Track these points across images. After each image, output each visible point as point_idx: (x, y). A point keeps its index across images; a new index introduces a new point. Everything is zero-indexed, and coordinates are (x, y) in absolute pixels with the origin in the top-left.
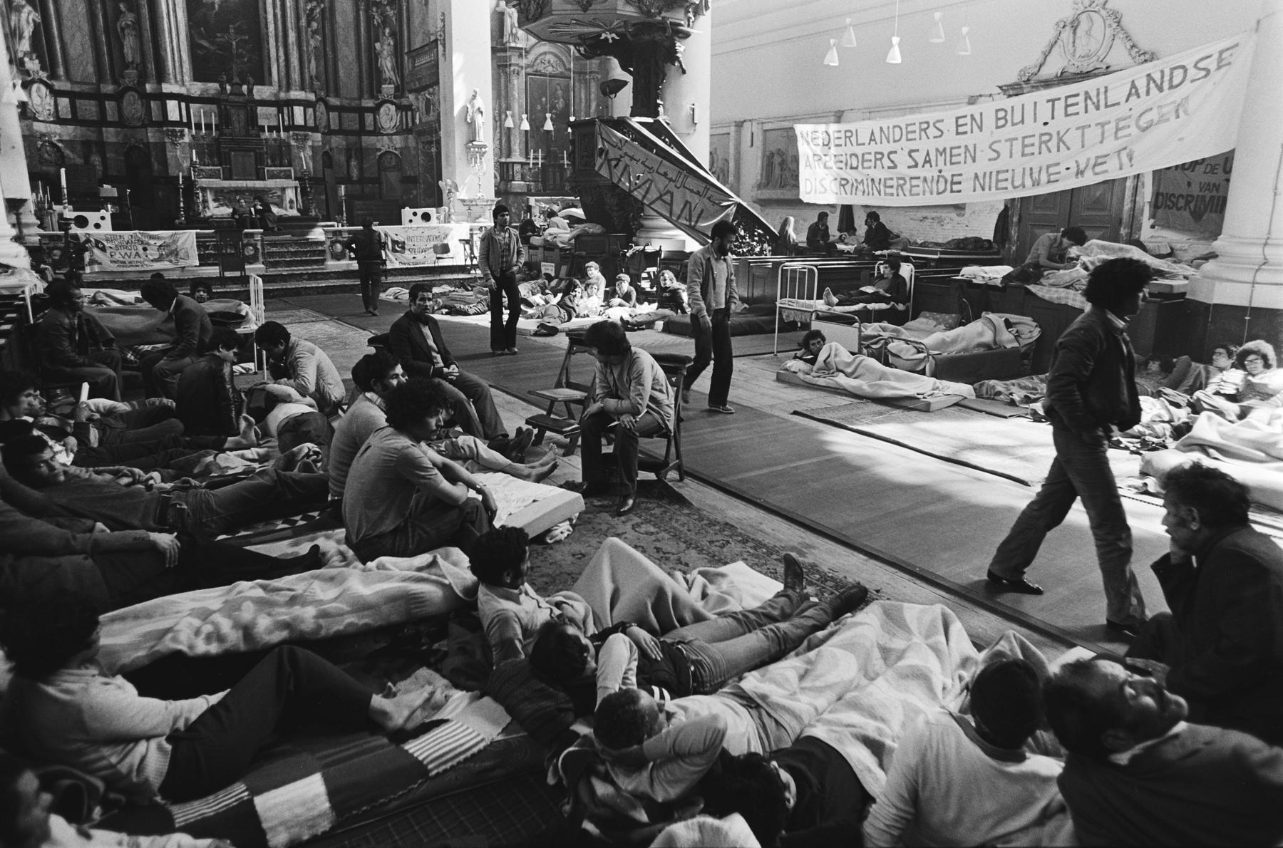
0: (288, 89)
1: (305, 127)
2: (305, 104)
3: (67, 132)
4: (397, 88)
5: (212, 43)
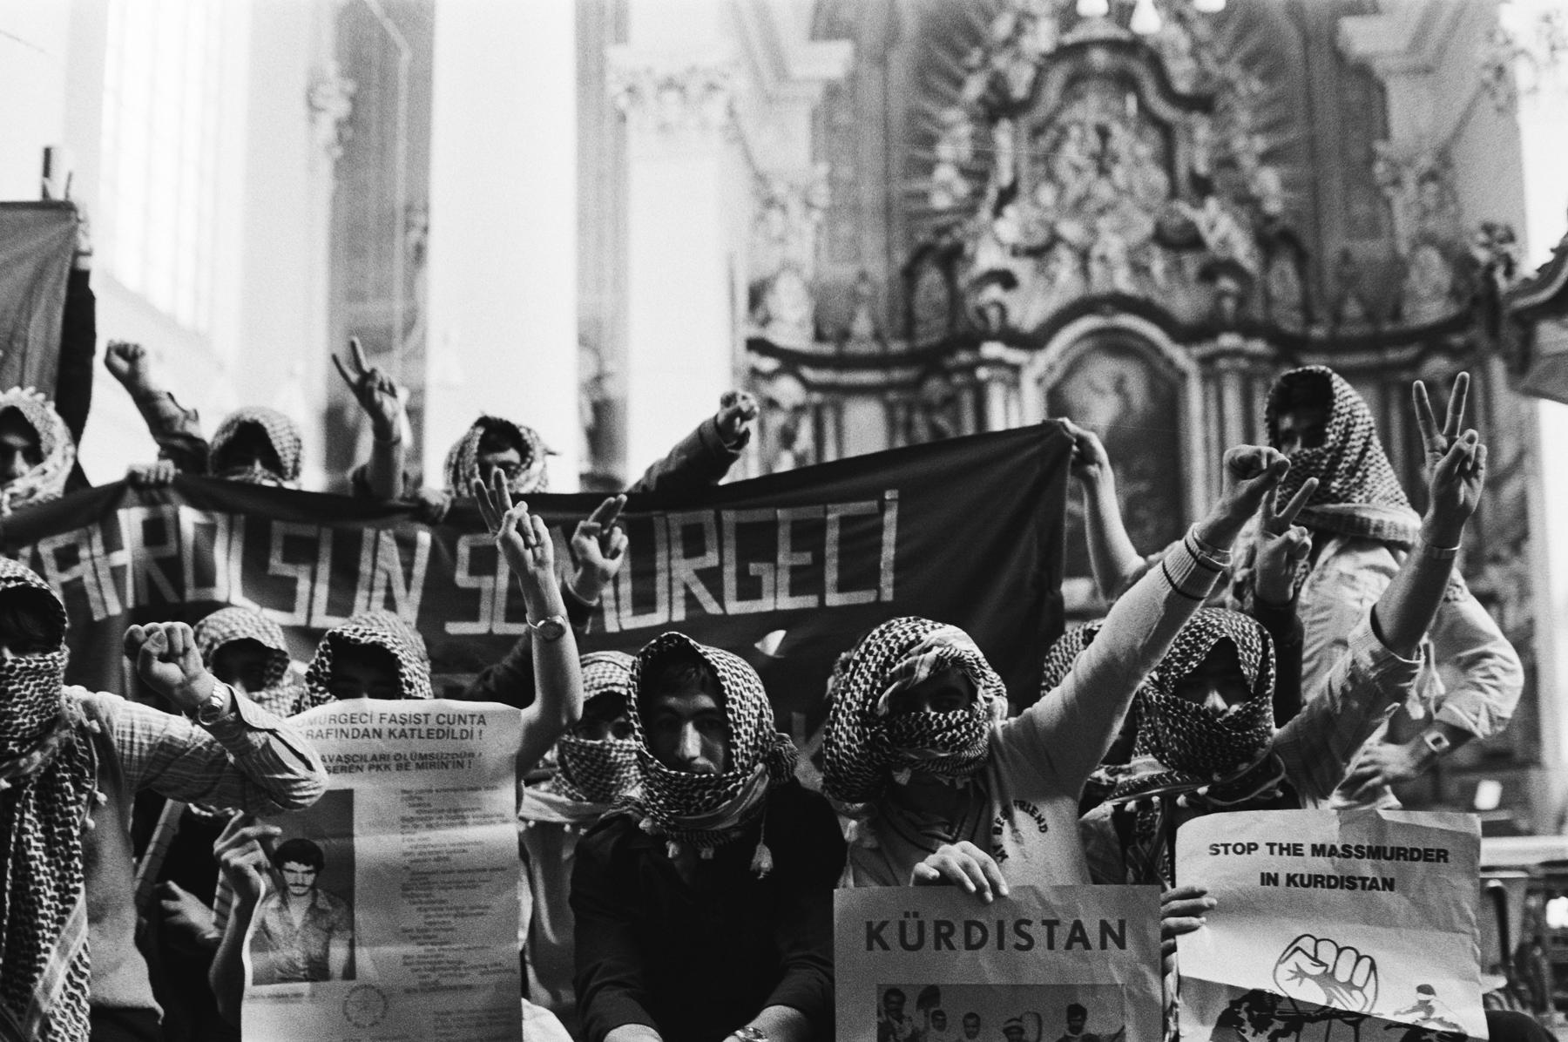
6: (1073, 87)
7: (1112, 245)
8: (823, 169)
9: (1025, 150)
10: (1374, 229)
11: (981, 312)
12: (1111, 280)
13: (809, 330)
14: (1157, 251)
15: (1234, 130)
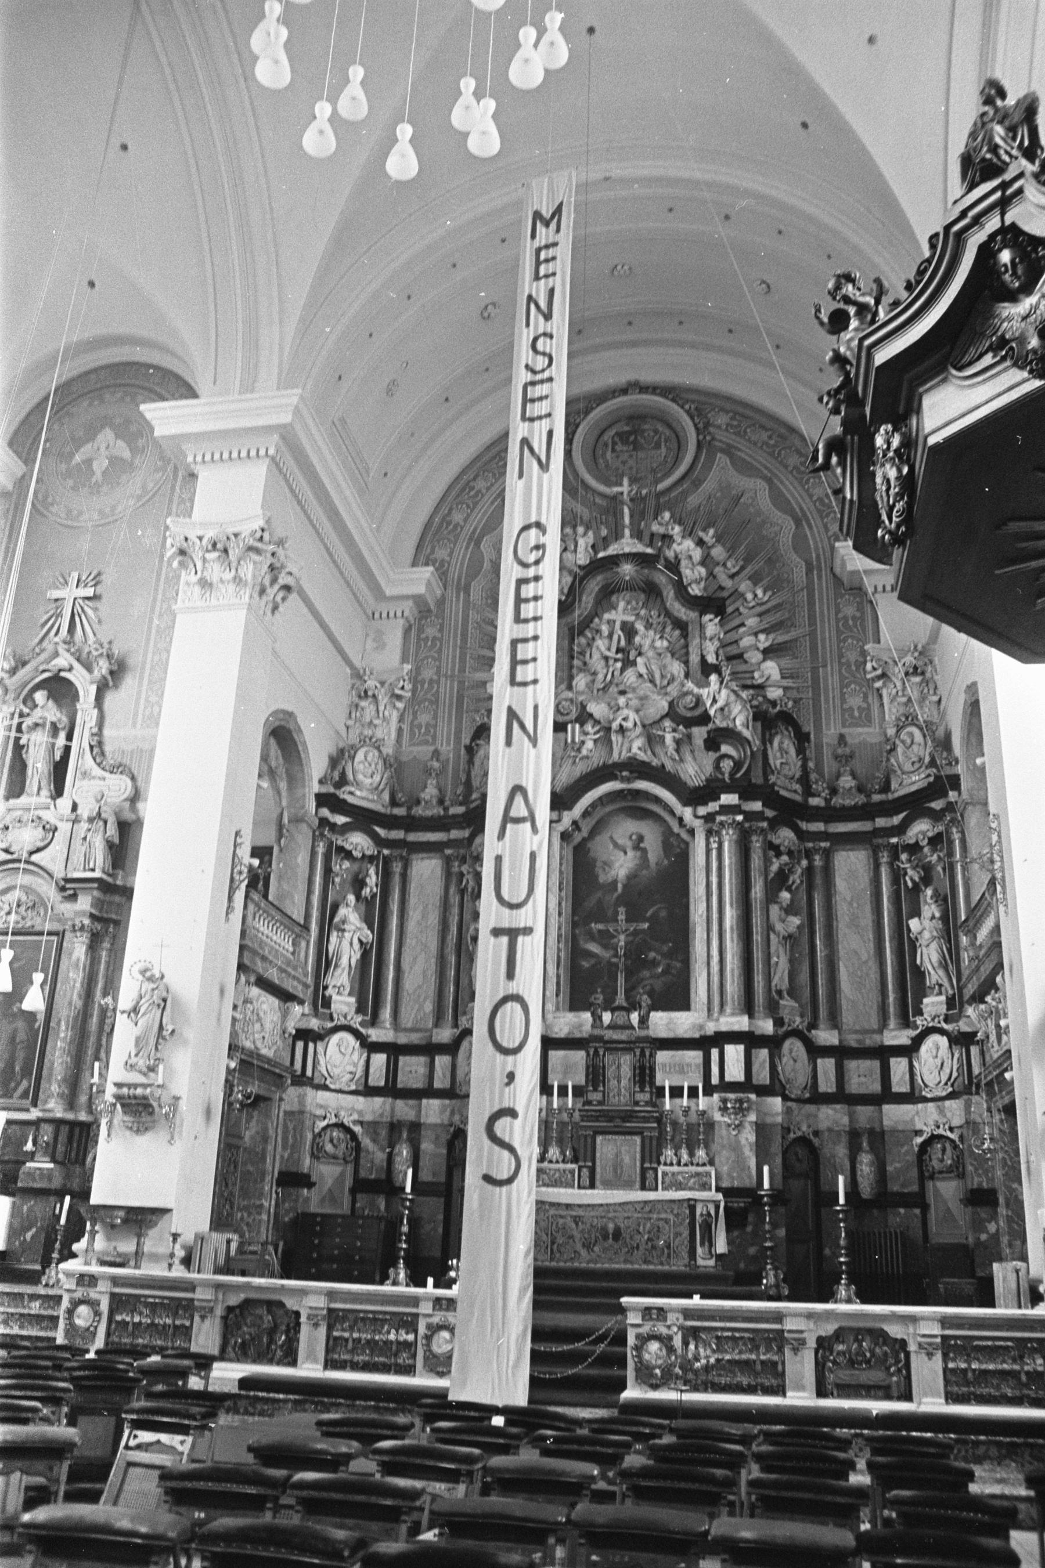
1: (747, 1085)
3: (374, 1107)
4: (950, 1003)
5: (605, 947)
8: (407, 667)
10: (866, 718)
12: (630, 750)
13: (386, 796)
14: (667, 723)
15: (742, 630)
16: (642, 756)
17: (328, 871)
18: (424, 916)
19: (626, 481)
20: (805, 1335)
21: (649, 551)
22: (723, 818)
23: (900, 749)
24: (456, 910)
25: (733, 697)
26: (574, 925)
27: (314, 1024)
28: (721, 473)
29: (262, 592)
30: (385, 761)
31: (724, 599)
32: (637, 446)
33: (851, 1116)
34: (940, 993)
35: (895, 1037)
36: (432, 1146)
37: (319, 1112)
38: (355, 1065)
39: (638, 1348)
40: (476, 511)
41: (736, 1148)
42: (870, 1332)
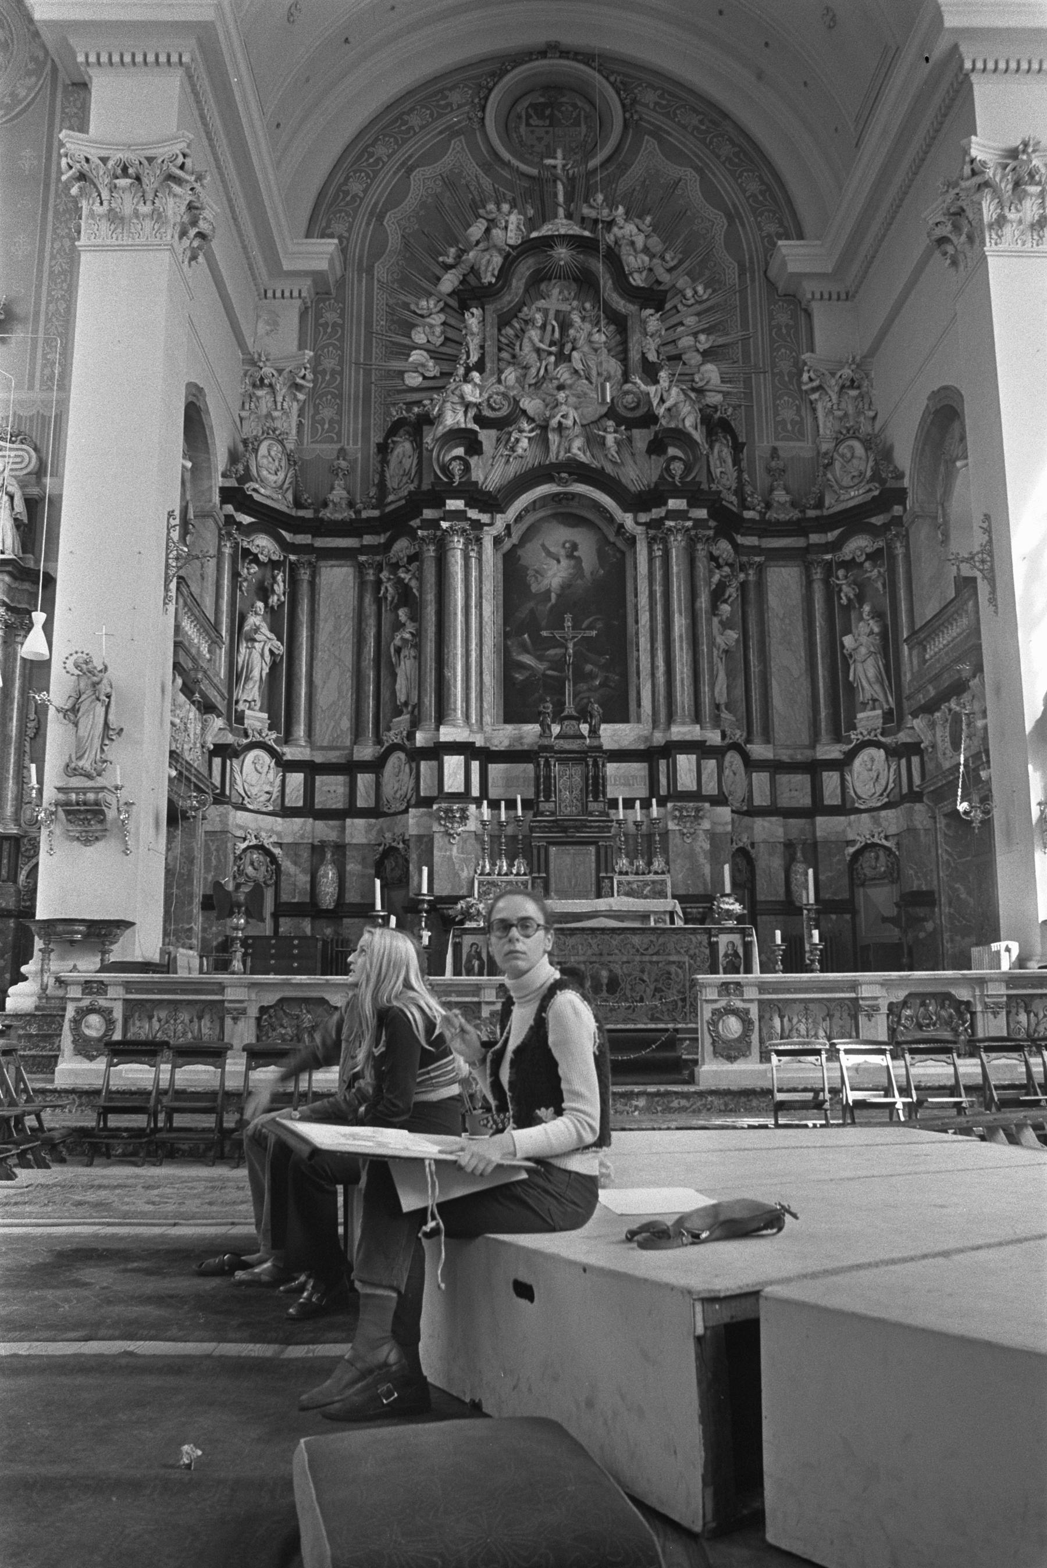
0: (670, 719)
1: (696, 796)
2: (699, 749)
4: (888, 716)
5: (540, 658)
6: (538, 280)
7: (569, 414)
9: (492, 331)
11: (445, 469)
12: (568, 450)
13: (290, 496)
15: (680, 329)
16: (583, 458)
17: (235, 575)
18: (337, 628)
19: (559, 154)
20: (880, 1001)
21: (587, 233)
22: (672, 523)
23: (837, 465)
24: (372, 622)
25: (682, 397)
26: (506, 635)
27: (230, 738)
28: (649, 157)
29: (183, 234)
30: (289, 455)
31: (666, 292)
32: (553, 122)
33: (785, 826)
34: (874, 709)
35: (826, 753)
36: (359, 867)
37: (240, 833)
38: (272, 784)
39: (713, 1023)
40: (377, 181)
41: (691, 856)
42: (933, 995)
